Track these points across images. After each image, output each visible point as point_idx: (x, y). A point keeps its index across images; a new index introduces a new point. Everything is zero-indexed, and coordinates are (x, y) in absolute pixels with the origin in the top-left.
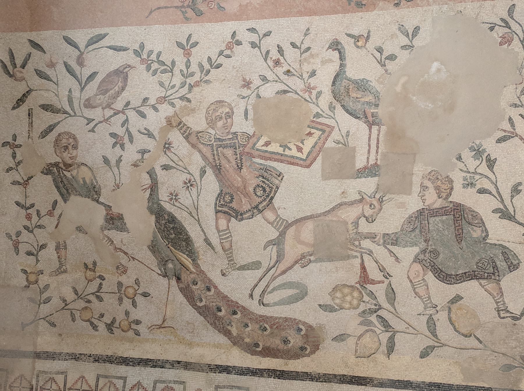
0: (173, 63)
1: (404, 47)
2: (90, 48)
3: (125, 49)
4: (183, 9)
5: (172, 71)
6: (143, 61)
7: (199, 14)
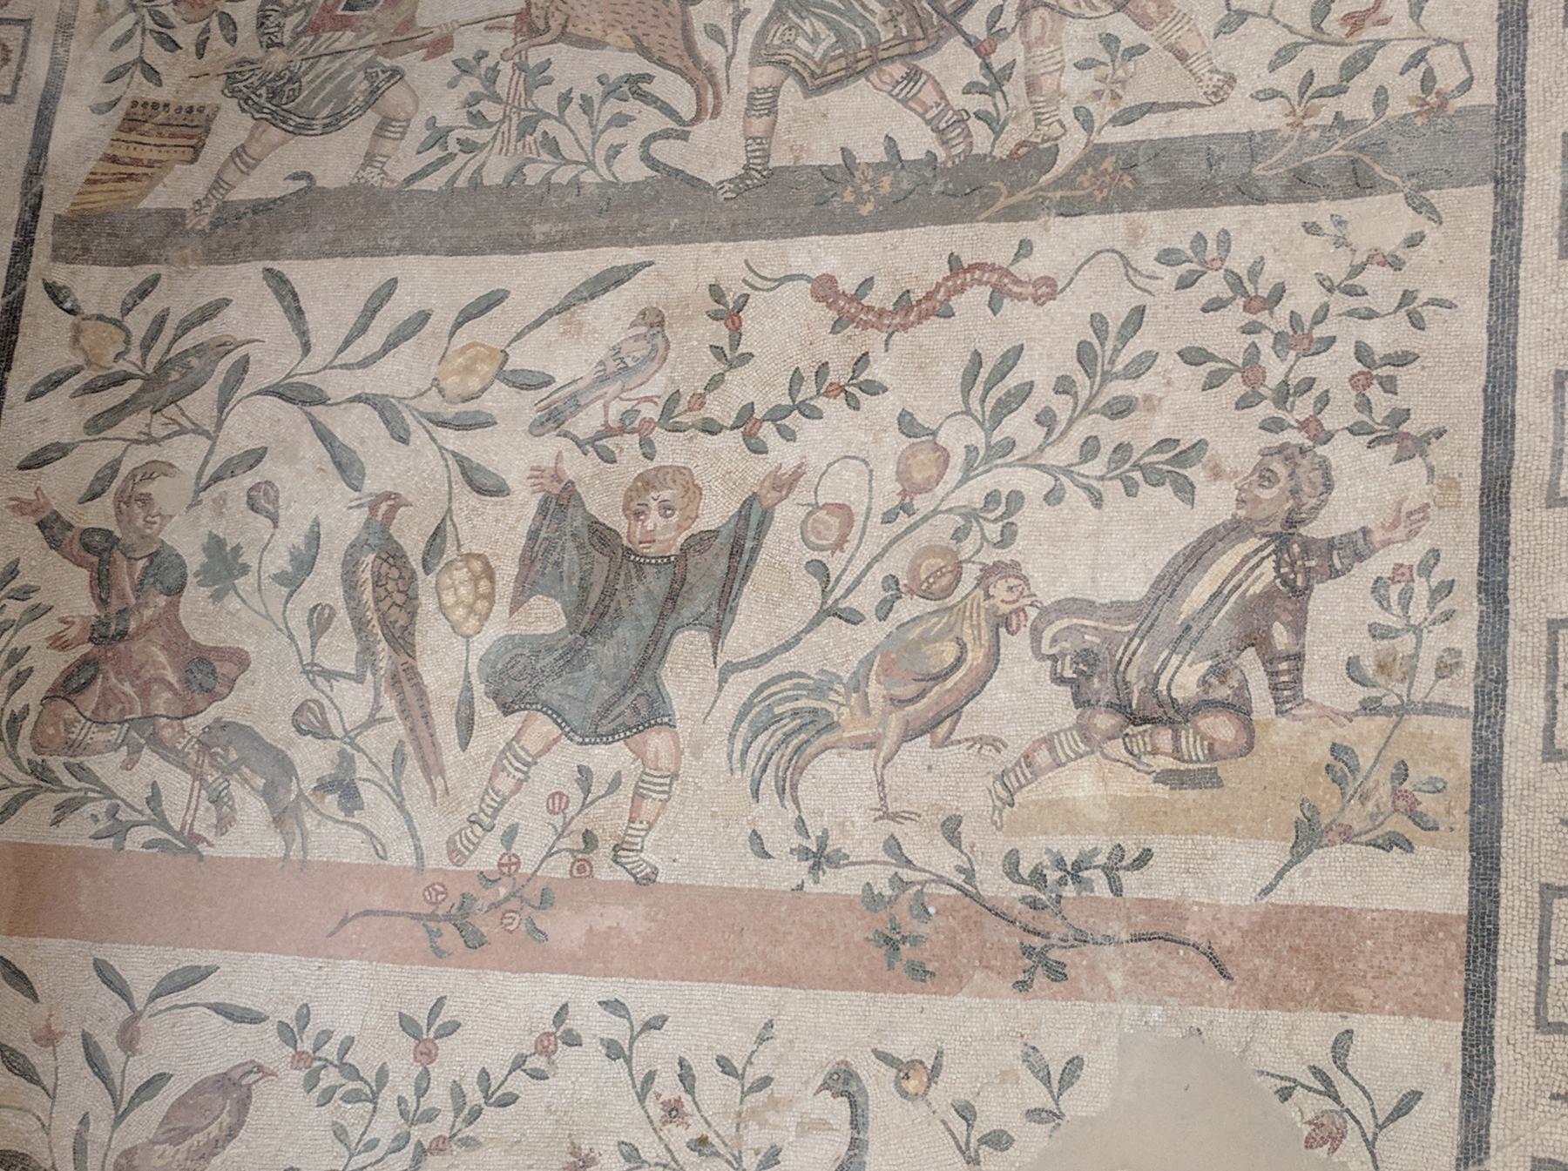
0: (382, 1075)
1: (1035, 1115)
2: (162, 1003)
3: (256, 1019)
4: (432, 924)
5: (374, 1099)
6: (299, 1058)
7: (475, 942)
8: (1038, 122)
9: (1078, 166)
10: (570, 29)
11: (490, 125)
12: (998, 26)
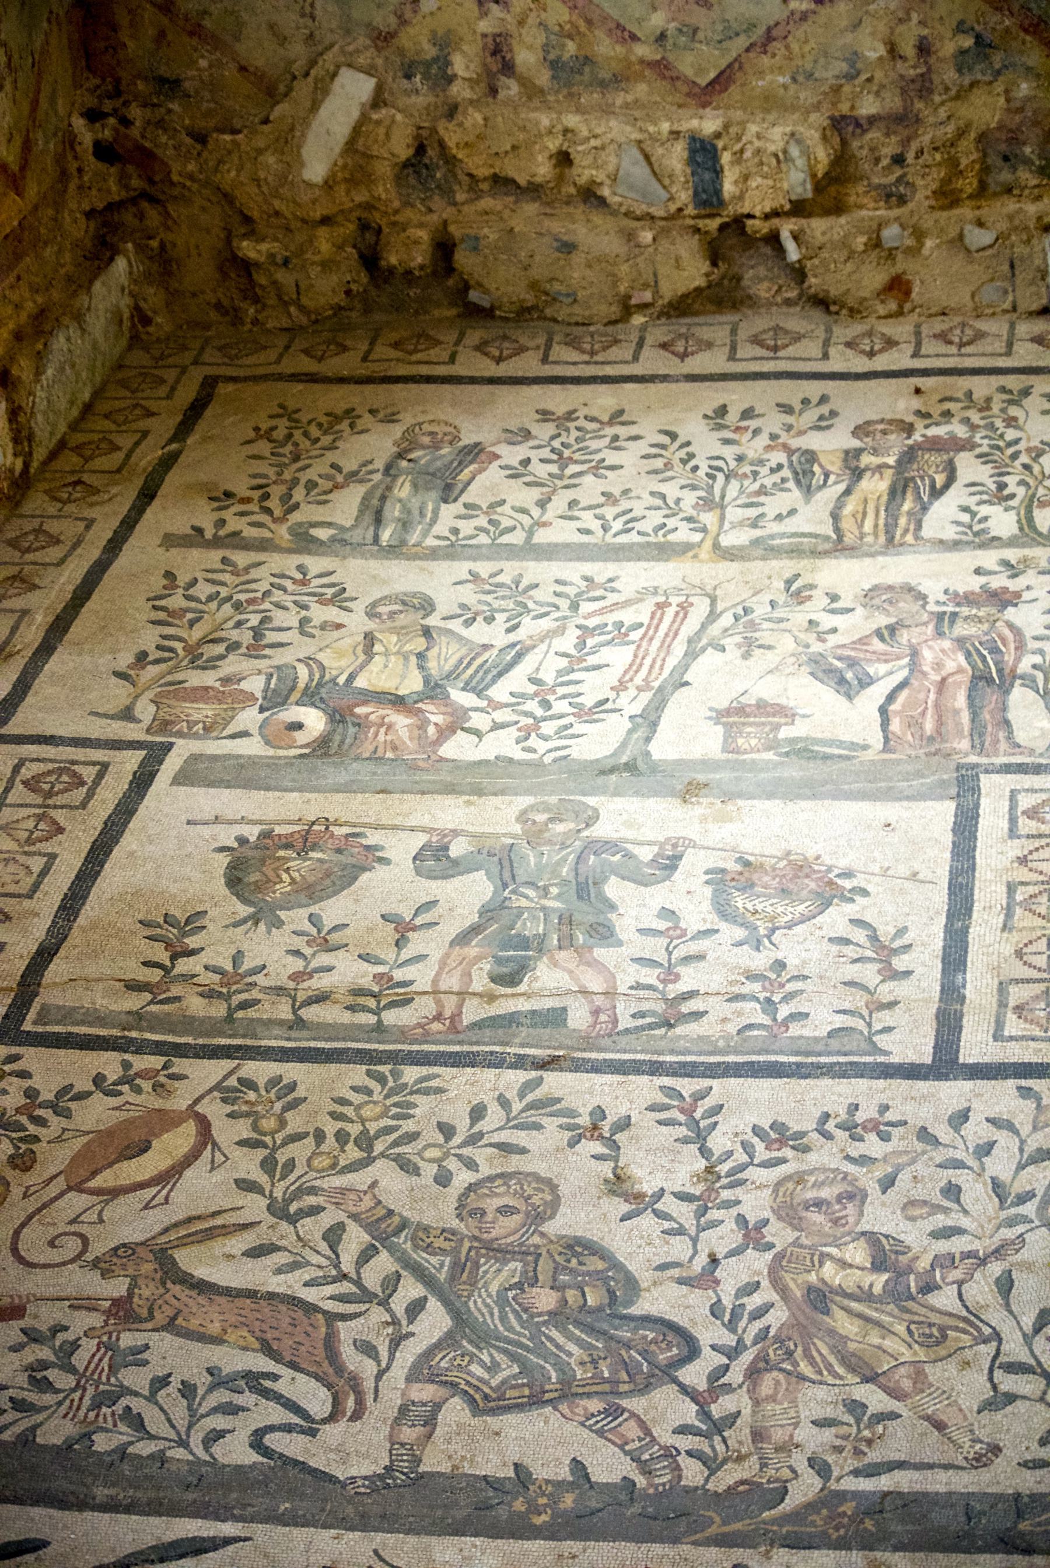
8: (763, 1466)
9: (811, 1507)
10: (180, 1321)
11: (57, 1391)
12: (722, 1381)
